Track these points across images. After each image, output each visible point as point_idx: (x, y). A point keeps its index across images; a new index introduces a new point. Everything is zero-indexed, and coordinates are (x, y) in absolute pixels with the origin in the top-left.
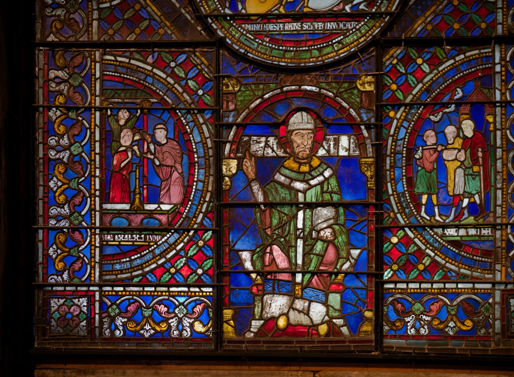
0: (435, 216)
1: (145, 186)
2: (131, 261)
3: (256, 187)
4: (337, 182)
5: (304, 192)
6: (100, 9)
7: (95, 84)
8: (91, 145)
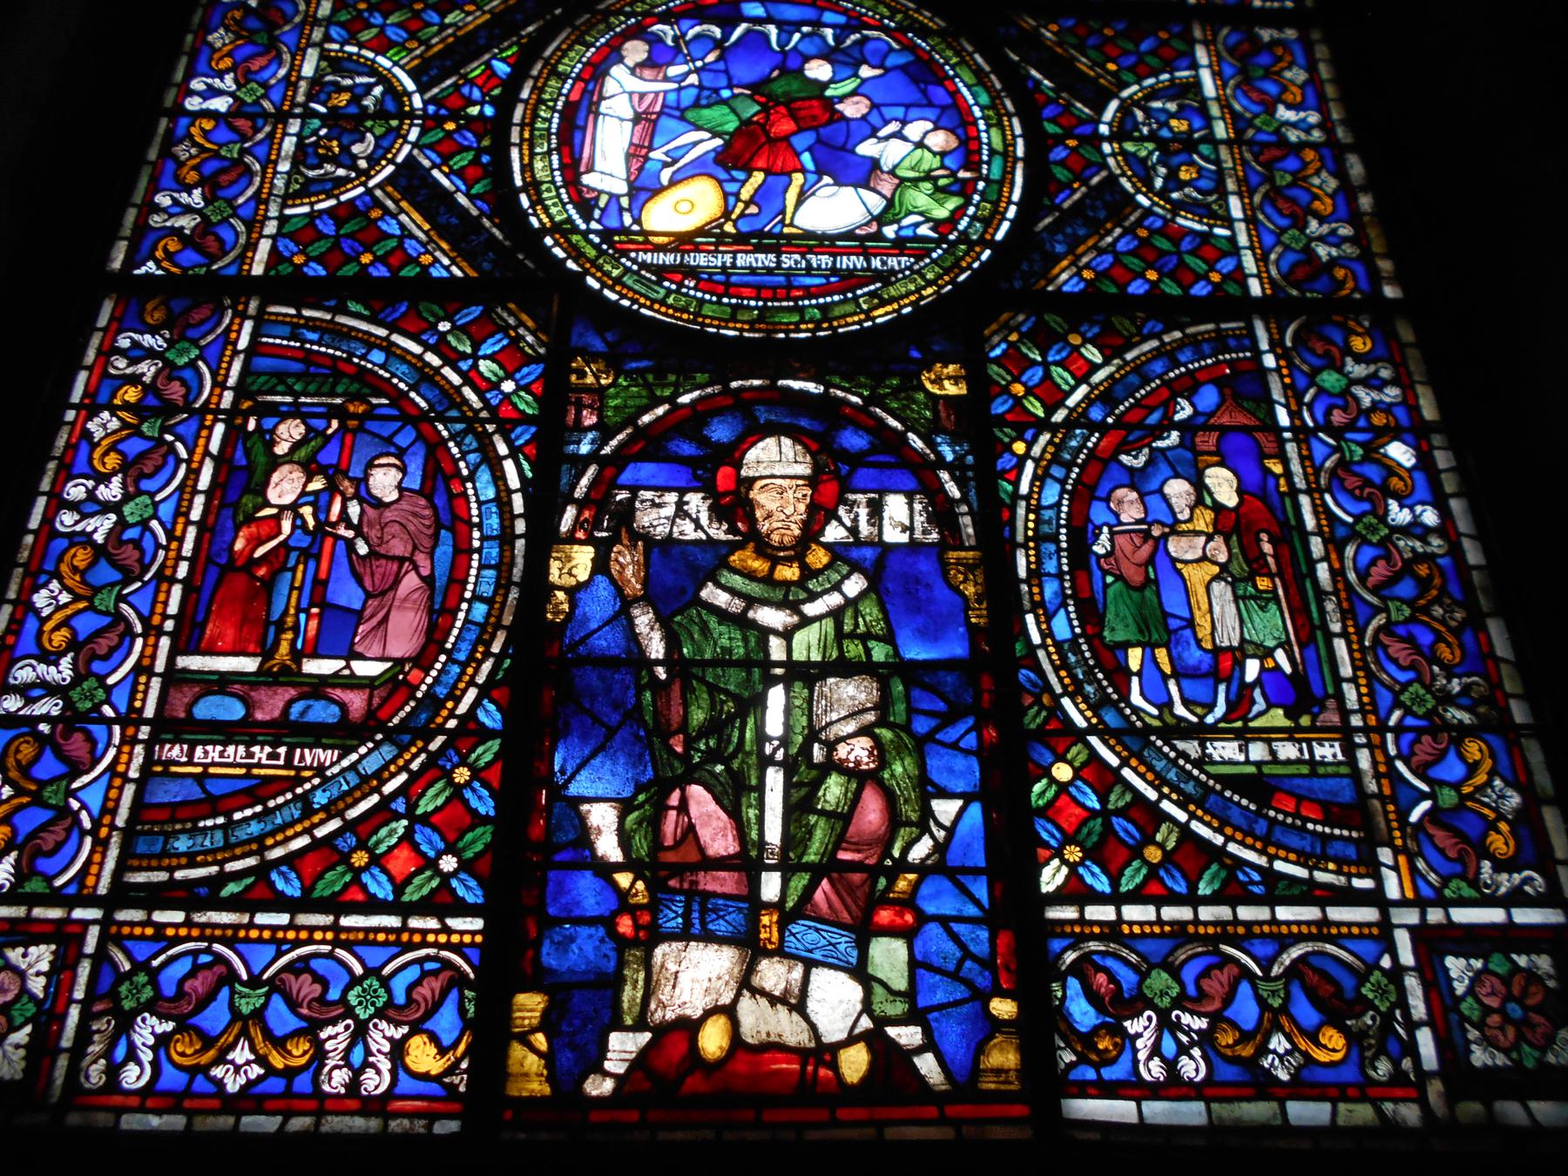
0: (1170, 704)
1: (315, 610)
2: (230, 825)
3: (643, 620)
4: (883, 610)
5: (787, 635)
6: (283, 220)
7: (230, 364)
8: (181, 499)
